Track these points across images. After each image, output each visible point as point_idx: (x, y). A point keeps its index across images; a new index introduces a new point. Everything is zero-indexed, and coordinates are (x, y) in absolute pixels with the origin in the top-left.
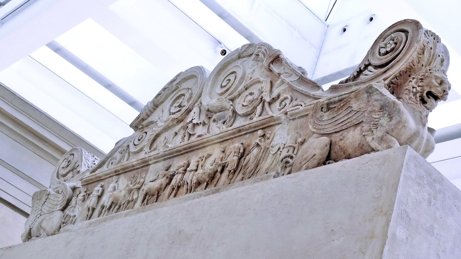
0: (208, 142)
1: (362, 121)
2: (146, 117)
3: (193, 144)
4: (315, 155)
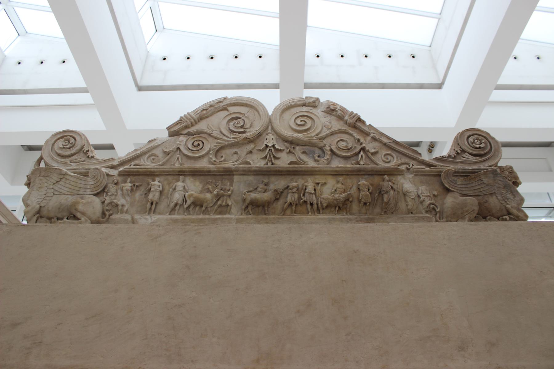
0: (319, 171)
1: (495, 193)
4: (474, 210)
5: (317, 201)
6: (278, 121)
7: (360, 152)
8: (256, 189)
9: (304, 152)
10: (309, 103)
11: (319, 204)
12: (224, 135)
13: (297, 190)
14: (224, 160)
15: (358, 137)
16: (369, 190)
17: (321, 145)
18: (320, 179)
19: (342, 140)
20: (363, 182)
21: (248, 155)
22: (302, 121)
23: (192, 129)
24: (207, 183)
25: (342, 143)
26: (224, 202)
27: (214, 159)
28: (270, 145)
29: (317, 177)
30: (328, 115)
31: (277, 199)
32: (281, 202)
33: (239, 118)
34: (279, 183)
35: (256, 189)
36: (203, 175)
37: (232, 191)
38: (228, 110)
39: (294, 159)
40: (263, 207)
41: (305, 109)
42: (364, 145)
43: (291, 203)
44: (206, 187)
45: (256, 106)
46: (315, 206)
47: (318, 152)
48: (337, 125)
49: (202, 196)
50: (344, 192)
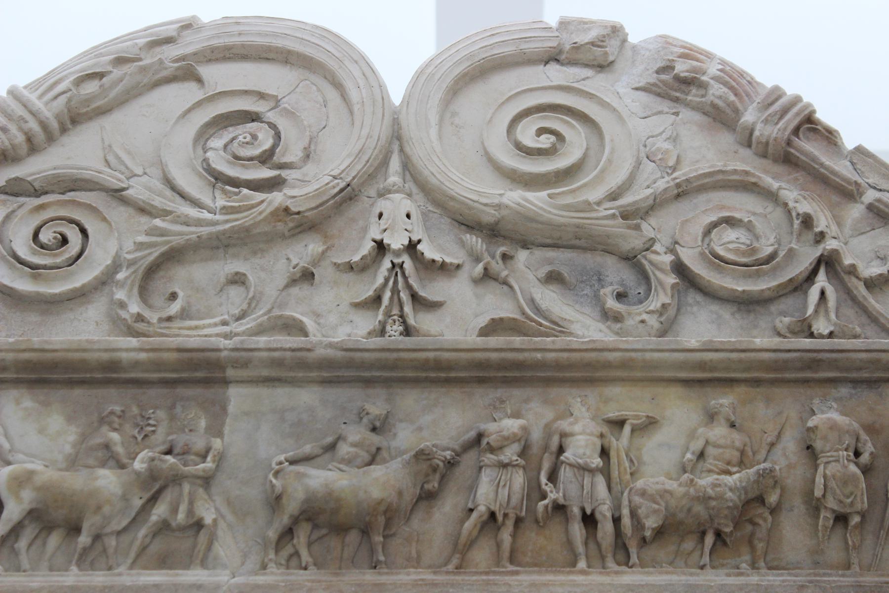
2: (25, 148)
3: (539, 356)
5: (617, 507)
6: (433, 132)
7: (814, 272)
8: (332, 447)
9: (553, 278)
10: (576, 48)
11: (626, 521)
12: (183, 196)
13: (523, 453)
14: (184, 314)
15: (805, 207)
16: (857, 454)
17: (633, 242)
18: (625, 401)
19: (730, 222)
20: (830, 415)
21: (295, 291)
22: (541, 131)
23: (32, 169)
24: (102, 421)
25: (731, 234)
26: (183, 508)
27: (135, 308)
28: (396, 242)
29: (615, 390)
30: (665, 106)
31: (427, 497)
32: (448, 507)
33: (253, 117)
34: (437, 422)
35: (332, 447)
36: (82, 382)
37: (220, 459)
38: (199, 80)
39: (506, 310)
40: (366, 531)
41: (556, 74)
42: (831, 244)
43: (492, 515)
44: (98, 440)
45: (331, 64)
46: (606, 528)
47: (617, 274)
48: (704, 151)
49: (76, 481)
50: (742, 464)
